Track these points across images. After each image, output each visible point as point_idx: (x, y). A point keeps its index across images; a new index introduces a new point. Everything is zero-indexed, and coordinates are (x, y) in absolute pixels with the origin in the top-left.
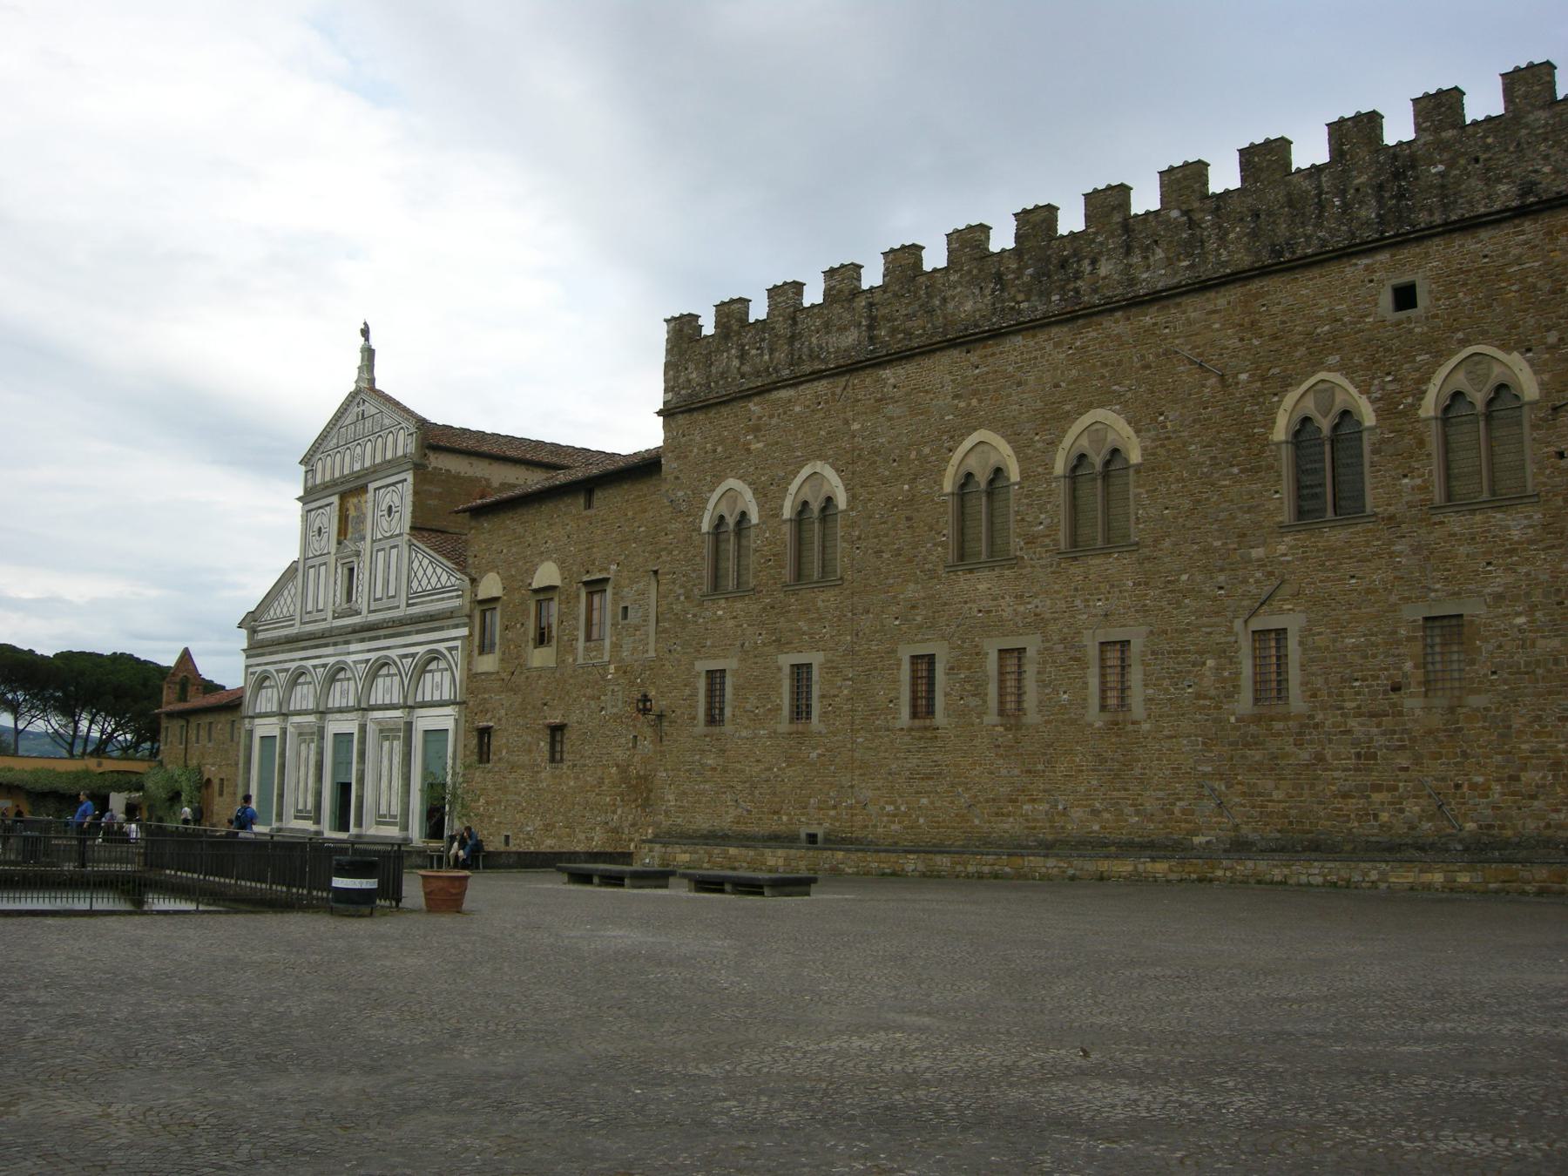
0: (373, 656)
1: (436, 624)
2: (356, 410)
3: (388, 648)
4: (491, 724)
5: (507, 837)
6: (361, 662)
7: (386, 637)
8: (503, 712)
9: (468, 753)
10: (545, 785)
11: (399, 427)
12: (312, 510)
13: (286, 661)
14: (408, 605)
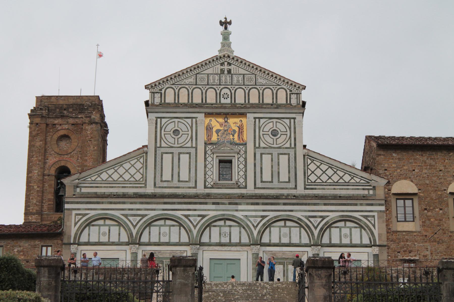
0: (272, 215)
1: (349, 202)
2: (219, 67)
3: (292, 211)
4: (417, 258)
6: (256, 217)
7: (285, 204)
8: (428, 253)
11: (279, 87)
12: (164, 118)
14: (305, 188)
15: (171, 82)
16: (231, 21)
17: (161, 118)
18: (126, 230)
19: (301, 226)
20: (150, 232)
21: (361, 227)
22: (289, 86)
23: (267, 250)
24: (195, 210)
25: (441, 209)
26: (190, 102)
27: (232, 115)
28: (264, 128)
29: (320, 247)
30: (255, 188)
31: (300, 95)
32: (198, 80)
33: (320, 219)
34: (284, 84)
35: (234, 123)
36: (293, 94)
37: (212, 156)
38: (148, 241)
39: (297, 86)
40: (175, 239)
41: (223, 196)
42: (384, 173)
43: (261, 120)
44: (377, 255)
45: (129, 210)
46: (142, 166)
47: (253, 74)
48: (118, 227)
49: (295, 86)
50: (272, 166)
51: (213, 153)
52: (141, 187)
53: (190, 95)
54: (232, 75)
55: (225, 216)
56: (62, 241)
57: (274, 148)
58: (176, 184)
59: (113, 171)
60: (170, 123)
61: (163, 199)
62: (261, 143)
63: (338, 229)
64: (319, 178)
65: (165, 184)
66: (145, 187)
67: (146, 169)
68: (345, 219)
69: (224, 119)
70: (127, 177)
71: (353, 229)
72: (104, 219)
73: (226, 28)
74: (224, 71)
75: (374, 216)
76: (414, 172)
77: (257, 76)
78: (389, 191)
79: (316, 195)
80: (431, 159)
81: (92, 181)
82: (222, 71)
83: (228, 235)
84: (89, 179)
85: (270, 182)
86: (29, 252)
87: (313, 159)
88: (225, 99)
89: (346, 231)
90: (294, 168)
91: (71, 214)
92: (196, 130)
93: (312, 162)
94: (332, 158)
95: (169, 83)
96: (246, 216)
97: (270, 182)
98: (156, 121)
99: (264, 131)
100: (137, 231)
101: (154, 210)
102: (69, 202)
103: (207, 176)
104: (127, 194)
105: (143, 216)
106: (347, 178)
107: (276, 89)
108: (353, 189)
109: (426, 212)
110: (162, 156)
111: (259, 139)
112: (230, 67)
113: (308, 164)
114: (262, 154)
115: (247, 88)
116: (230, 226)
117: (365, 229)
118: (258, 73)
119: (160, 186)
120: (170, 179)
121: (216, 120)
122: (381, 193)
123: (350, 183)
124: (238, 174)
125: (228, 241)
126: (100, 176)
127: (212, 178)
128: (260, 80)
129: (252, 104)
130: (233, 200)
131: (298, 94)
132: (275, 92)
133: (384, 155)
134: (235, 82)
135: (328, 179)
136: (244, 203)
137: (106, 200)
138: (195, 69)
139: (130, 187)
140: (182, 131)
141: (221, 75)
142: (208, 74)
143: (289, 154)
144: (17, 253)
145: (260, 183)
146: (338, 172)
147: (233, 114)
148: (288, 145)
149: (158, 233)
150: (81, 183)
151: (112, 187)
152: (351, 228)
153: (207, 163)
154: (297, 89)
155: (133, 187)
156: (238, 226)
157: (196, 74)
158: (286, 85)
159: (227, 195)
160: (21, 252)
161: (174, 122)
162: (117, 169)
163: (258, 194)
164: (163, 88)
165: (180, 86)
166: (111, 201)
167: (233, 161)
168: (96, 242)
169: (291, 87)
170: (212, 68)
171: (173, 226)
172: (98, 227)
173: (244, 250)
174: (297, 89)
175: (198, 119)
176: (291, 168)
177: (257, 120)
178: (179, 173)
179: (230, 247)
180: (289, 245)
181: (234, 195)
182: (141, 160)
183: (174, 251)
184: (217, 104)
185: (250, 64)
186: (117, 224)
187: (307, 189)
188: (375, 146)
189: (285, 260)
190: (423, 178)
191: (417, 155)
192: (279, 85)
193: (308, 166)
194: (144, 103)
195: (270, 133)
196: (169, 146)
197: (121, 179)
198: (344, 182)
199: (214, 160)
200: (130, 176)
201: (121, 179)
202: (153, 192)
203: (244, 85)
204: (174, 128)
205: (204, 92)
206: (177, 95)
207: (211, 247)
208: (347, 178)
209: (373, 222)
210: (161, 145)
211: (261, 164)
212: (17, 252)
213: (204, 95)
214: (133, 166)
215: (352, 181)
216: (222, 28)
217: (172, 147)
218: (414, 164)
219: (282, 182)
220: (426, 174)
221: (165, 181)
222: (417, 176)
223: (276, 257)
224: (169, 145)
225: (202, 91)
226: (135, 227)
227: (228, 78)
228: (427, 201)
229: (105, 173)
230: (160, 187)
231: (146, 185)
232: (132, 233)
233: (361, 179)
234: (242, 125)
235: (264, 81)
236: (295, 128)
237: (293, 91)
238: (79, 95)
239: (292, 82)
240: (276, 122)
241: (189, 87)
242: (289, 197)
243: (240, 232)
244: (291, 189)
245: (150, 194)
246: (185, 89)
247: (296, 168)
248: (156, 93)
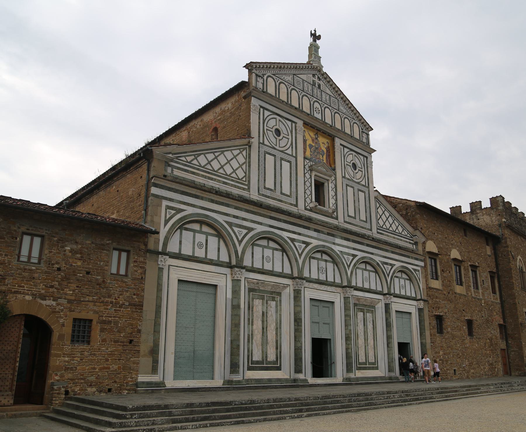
0: (360, 255)
3: (372, 254)
5: (455, 370)
6: (348, 254)
7: (368, 245)
9: (431, 327)
10: (468, 345)
11: (354, 121)
12: (267, 110)
13: (244, 219)
16: (320, 36)
17: (264, 109)
18: (226, 245)
19: (376, 272)
20: (253, 253)
23: (354, 295)
24: (300, 234)
27: (322, 134)
29: (392, 296)
30: (345, 222)
41: (322, 223)
44: (423, 309)
45: (235, 217)
46: (244, 161)
47: (336, 98)
48: (217, 238)
50: (354, 201)
52: (244, 189)
55: (325, 248)
56: (146, 245)
62: (346, 173)
65: (268, 193)
67: (249, 166)
69: (315, 135)
70: (228, 170)
72: (201, 223)
73: (315, 41)
75: (419, 271)
81: (187, 162)
82: (314, 84)
84: (183, 159)
86: (91, 256)
91: (160, 205)
92: (296, 137)
96: (341, 251)
98: (260, 110)
101: (260, 224)
102: (158, 184)
104: (231, 195)
105: (250, 230)
108: (404, 241)
110: (265, 156)
111: (344, 168)
112: (319, 82)
116: (326, 261)
117: (412, 283)
128: (341, 108)
137: (207, 195)
139: (232, 185)
142: (303, 80)
144: (70, 254)
147: (323, 133)
148: (363, 183)
151: (212, 179)
152: (405, 279)
155: (235, 186)
157: (294, 74)
159: (326, 223)
160: (76, 253)
166: (213, 198)
167: (326, 184)
168: (189, 256)
171: (277, 249)
172: (192, 233)
173: (338, 292)
175: (297, 125)
178: (281, 182)
179: (326, 286)
180: (369, 291)
181: (331, 224)
182: (244, 153)
183: (278, 284)
186: (216, 233)
187: (378, 233)
189: (364, 307)
193: (377, 209)
201: (221, 171)
203: (330, 106)
207: (311, 284)
211: (347, 197)
212: (70, 252)
215: (403, 233)
217: (275, 149)
223: (358, 303)
224: (272, 145)
225: (299, 95)
226: (240, 242)
229: (203, 156)
230: (263, 195)
231: (249, 188)
232: (237, 251)
235: (344, 109)
242: (370, 238)
243: (334, 269)
247: (370, 208)
248: (259, 76)
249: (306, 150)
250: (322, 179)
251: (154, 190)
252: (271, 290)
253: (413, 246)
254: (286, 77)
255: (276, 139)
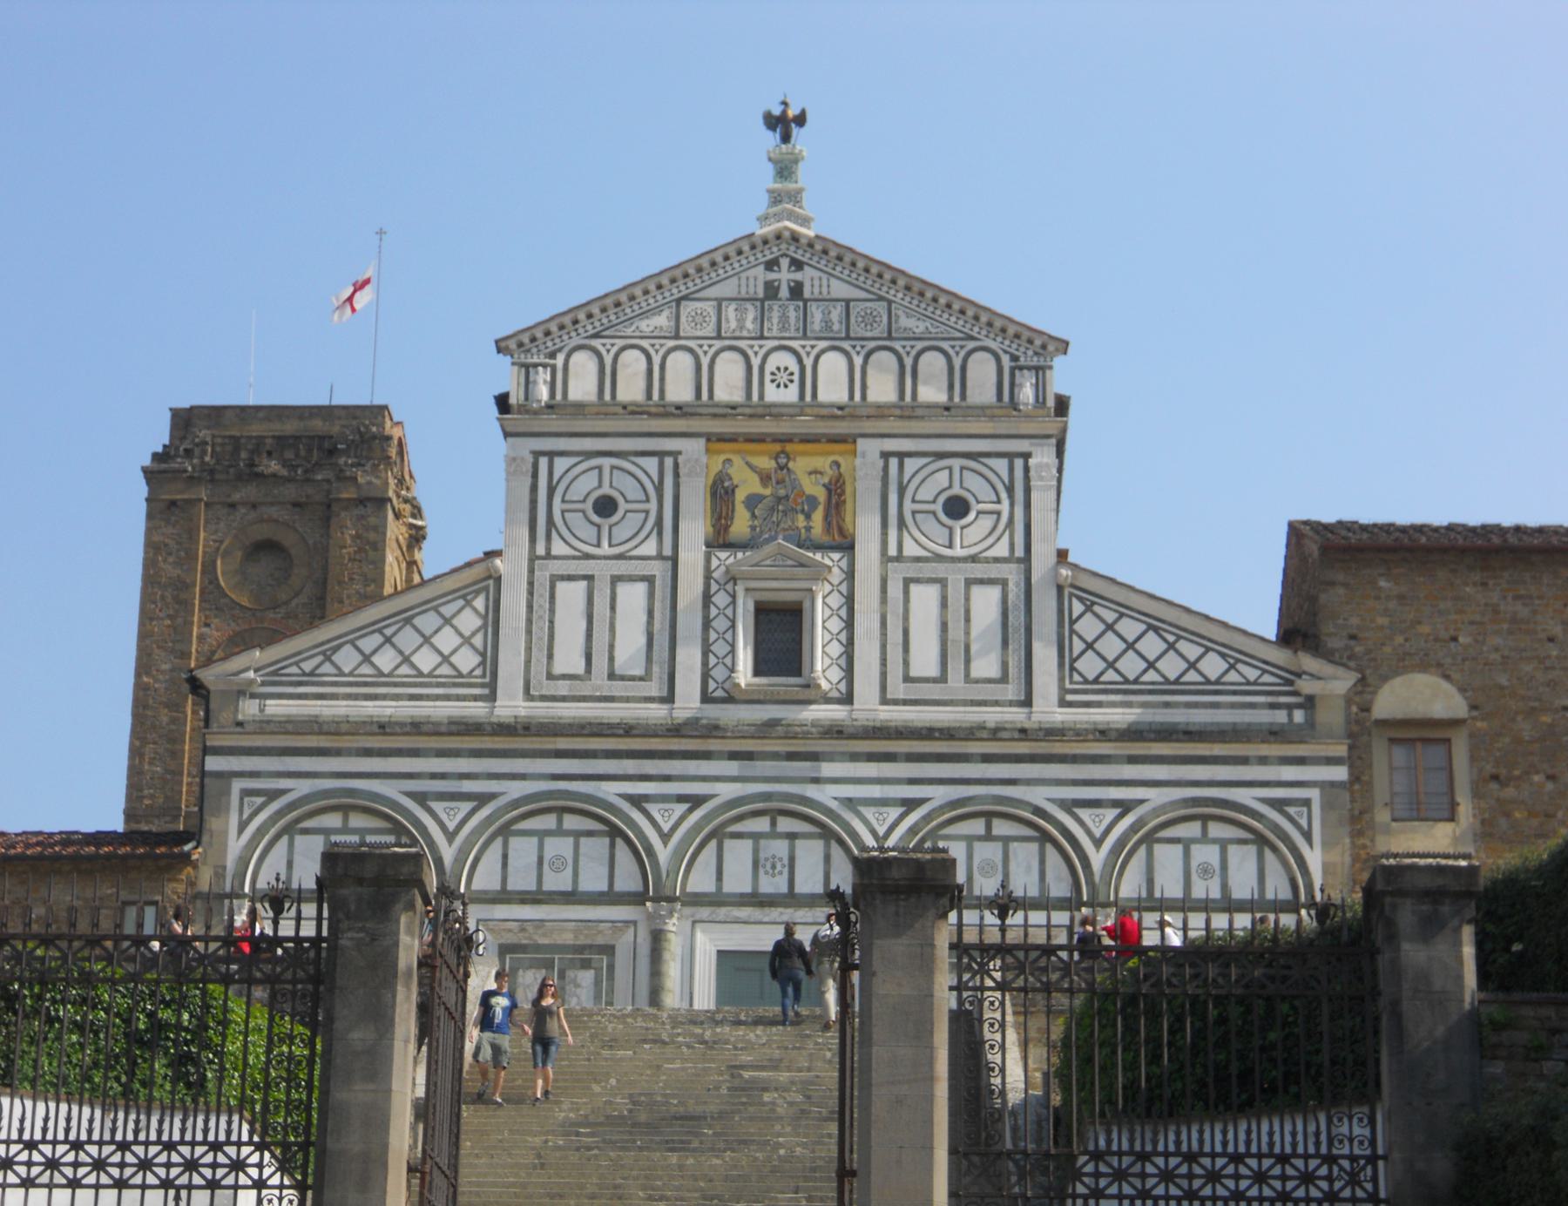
0: (940, 794)
6: (884, 802)
7: (987, 758)
11: (971, 345)
12: (562, 454)
14: (1063, 703)
15: (589, 327)
17: (551, 455)
19: (1045, 837)
20: (505, 857)
21: (1261, 841)
22: (1007, 342)
24: (667, 778)
25: (1551, 778)
26: (656, 396)
28: (917, 489)
30: (884, 701)
31: (1048, 372)
32: (683, 319)
33: (1111, 814)
34: (992, 335)
35: (810, 473)
36: (1021, 368)
37: (729, 587)
38: (499, 888)
39: (1038, 342)
40: (594, 881)
42: (1347, 648)
43: (907, 461)
45: (434, 776)
47: (881, 298)
49: (1030, 342)
50: (944, 627)
51: (734, 580)
52: (476, 698)
53: (654, 375)
54: (806, 301)
56: (192, 884)
57: (954, 560)
58: (599, 688)
59: (377, 639)
60: (584, 472)
61: (552, 739)
62: (908, 541)
63: (1178, 849)
64: (1111, 665)
65: (563, 688)
66: (492, 697)
68: (1204, 812)
69: (776, 458)
71: (1232, 849)
72: (345, 810)
74: (779, 287)
75: (1307, 803)
76: (1452, 645)
77: (893, 305)
78: (1365, 714)
79: (1100, 727)
80: (1517, 598)
81: (304, 674)
82: (771, 290)
83: (784, 866)
84: (294, 670)
85: (934, 680)
87: (1091, 601)
88: (778, 386)
89: (1206, 854)
90: (1023, 630)
91: (228, 793)
93: (1089, 608)
94: (1158, 594)
95: (581, 331)
96: (850, 800)
97: (934, 680)
99: (917, 498)
100: (460, 850)
101: (522, 777)
103: (712, 660)
106: (1213, 666)
107: (962, 353)
108: (1233, 706)
109: (1494, 786)
112: (798, 276)
113: (1075, 616)
114: (907, 582)
115: (858, 348)
116: (792, 836)
117: (1274, 849)
118: (900, 295)
119: (544, 692)
120: (580, 669)
121: (747, 463)
122: (1332, 716)
123: (1224, 684)
124: (823, 652)
125: (784, 889)
126: (333, 658)
127: (729, 664)
128: (905, 322)
129: (879, 406)
130: (805, 745)
131: (1040, 371)
132: (957, 362)
133: (1346, 585)
134: (817, 327)
135: (1145, 671)
136: (843, 753)
138: (673, 281)
139: (437, 698)
140: (627, 501)
141: (766, 303)
142: (719, 302)
143: (1004, 583)
145: (902, 685)
146: (1182, 646)
148: (1002, 550)
149: (536, 859)
150: (263, 684)
152: (1223, 844)
153: (713, 611)
154: (1036, 353)
155: (447, 698)
156: (820, 836)
157: (678, 301)
158: (999, 339)
161: (600, 468)
162: (395, 634)
163: (893, 724)
164: (560, 350)
165: (620, 343)
167: (806, 605)
169: (1014, 346)
170: (735, 280)
171: (590, 834)
174: (1036, 353)
175: (681, 459)
176: (1010, 630)
177: (894, 462)
178: (612, 647)
179: (790, 910)
182: (479, 603)
184: (749, 406)
185: (870, 263)
187: (1071, 704)
188: (1316, 554)
190: (1485, 664)
191: (1467, 585)
192: (972, 338)
193: (1072, 622)
194: (493, 401)
195: (938, 507)
196: (577, 554)
197: (405, 670)
198: (1200, 679)
199: (740, 601)
200: (439, 659)
201: (405, 670)
202: (523, 713)
203: (848, 337)
204: (595, 489)
205: (705, 361)
206: (607, 375)
208: (1213, 666)
209: (1304, 823)
210: (548, 549)
211: (906, 618)
213: (702, 376)
214: (447, 621)
215: (1233, 676)
216: (771, 139)
217: (587, 556)
218: (1453, 617)
219: (977, 681)
220: (1497, 650)
221: (564, 677)
222: (1464, 660)
224: (579, 551)
227: (792, 314)
228: (1499, 750)
229: (348, 647)
233: (1264, 671)
234: (838, 481)
236: (1027, 490)
237: (1022, 359)
238: (326, 403)
239: (1019, 329)
240: (962, 468)
241: (653, 345)
243: (827, 859)
244: (1011, 704)
245: (507, 721)
246: (636, 353)
249: (732, 518)
250: (783, 593)
251: (213, 763)
252: (578, 943)
253: (1290, 716)
254: (646, 325)
255: (599, 527)
